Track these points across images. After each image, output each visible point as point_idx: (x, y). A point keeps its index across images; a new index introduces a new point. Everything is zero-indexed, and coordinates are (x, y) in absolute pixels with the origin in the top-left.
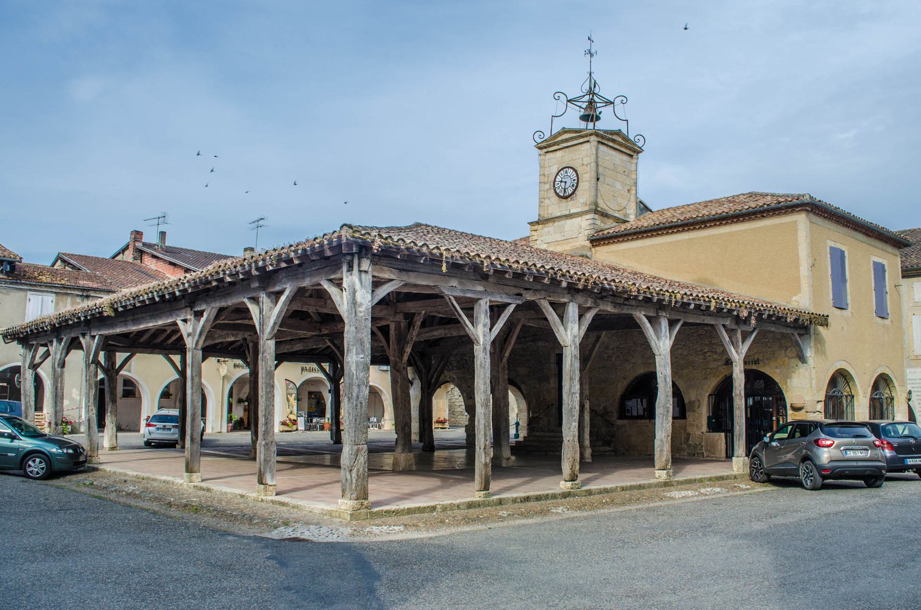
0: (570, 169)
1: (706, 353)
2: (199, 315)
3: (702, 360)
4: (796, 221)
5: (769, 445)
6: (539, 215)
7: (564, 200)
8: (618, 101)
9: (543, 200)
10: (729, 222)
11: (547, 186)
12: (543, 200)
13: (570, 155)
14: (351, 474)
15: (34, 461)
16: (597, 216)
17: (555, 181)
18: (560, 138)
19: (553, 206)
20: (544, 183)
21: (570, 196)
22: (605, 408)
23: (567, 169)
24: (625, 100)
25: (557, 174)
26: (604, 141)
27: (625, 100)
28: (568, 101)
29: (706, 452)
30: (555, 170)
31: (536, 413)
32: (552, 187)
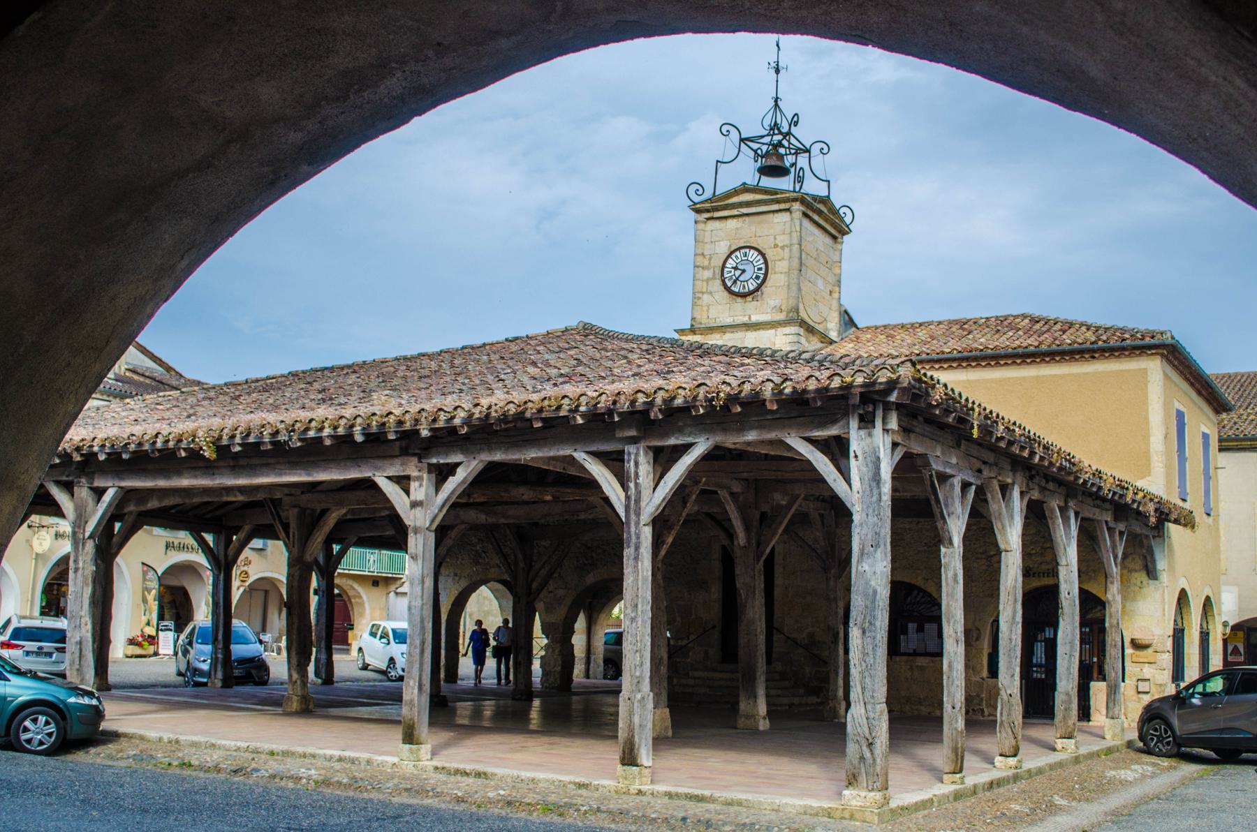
0: (752, 251)
1: (992, 556)
2: (443, 473)
3: (984, 567)
4: (1145, 370)
5: (1187, 702)
6: (693, 319)
7: (739, 299)
8: (815, 150)
9: (700, 295)
10: (1038, 360)
11: (707, 274)
12: (700, 295)
13: (753, 228)
14: (871, 750)
15: (35, 721)
16: (802, 331)
17: (724, 266)
18: (735, 200)
19: (720, 307)
20: (703, 268)
21: (751, 293)
22: (811, 635)
23: (747, 250)
24: (825, 151)
25: (729, 256)
26: (811, 214)
27: (826, 149)
28: (742, 140)
29: (987, 707)
30: (722, 248)
31: (682, 639)
32: (718, 276)
